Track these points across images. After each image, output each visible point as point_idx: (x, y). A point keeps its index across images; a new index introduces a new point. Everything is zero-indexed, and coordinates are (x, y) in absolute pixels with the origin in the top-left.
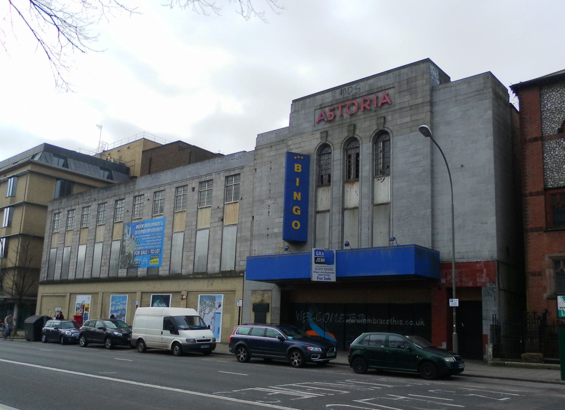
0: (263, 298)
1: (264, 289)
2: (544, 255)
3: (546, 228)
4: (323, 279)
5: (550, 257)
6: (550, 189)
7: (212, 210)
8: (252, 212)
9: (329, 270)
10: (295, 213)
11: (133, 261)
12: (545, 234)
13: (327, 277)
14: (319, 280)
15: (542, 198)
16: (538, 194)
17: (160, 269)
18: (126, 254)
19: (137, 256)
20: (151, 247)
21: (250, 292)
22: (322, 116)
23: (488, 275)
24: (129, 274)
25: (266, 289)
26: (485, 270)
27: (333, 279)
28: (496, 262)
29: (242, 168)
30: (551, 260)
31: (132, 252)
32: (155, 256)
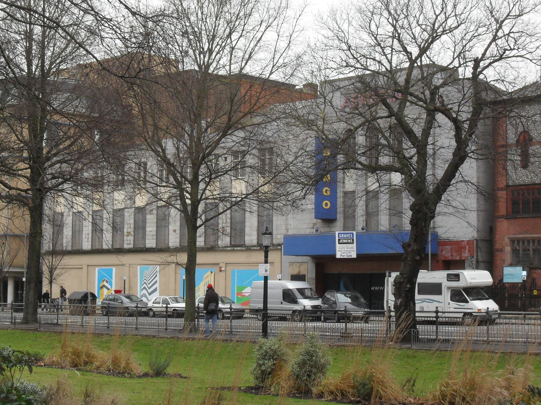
0: (300, 269)
1: (300, 261)
2: (504, 236)
3: (507, 216)
4: (346, 256)
5: (508, 238)
6: (511, 186)
9: (350, 248)
10: (325, 194)
12: (505, 221)
13: (349, 254)
14: (342, 257)
15: (505, 192)
16: (502, 189)
21: (288, 265)
22: (347, 102)
23: (469, 251)
25: (302, 261)
26: (467, 247)
27: (354, 255)
28: (475, 242)
30: (509, 240)
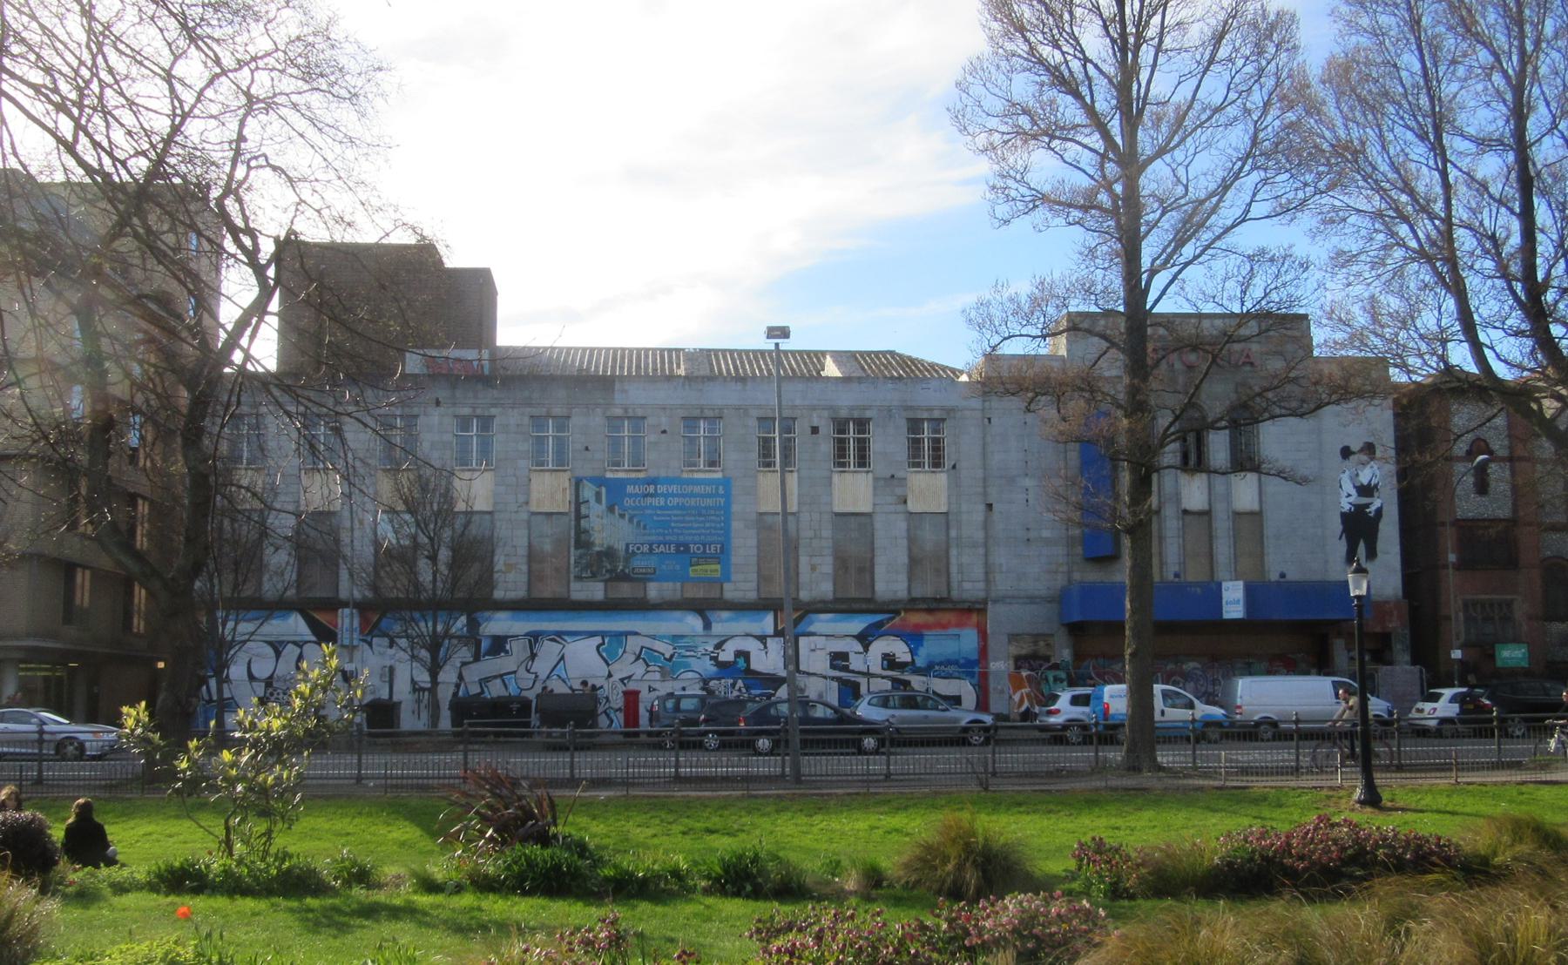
7: (876, 479)
8: (985, 494)
11: (625, 567)
17: (726, 586)
18: (597, 549)
19: (639, 557)
20: (690, 538)
21: (1005, 639)
24: (611, 595)
26: (1395, 613)
29: (951, 411)
31: (620, 546)
32: (705, 558)
